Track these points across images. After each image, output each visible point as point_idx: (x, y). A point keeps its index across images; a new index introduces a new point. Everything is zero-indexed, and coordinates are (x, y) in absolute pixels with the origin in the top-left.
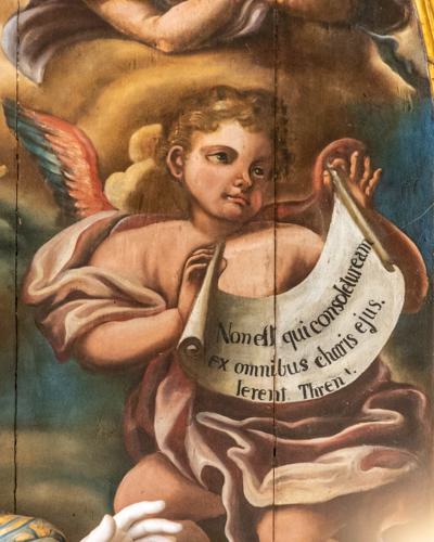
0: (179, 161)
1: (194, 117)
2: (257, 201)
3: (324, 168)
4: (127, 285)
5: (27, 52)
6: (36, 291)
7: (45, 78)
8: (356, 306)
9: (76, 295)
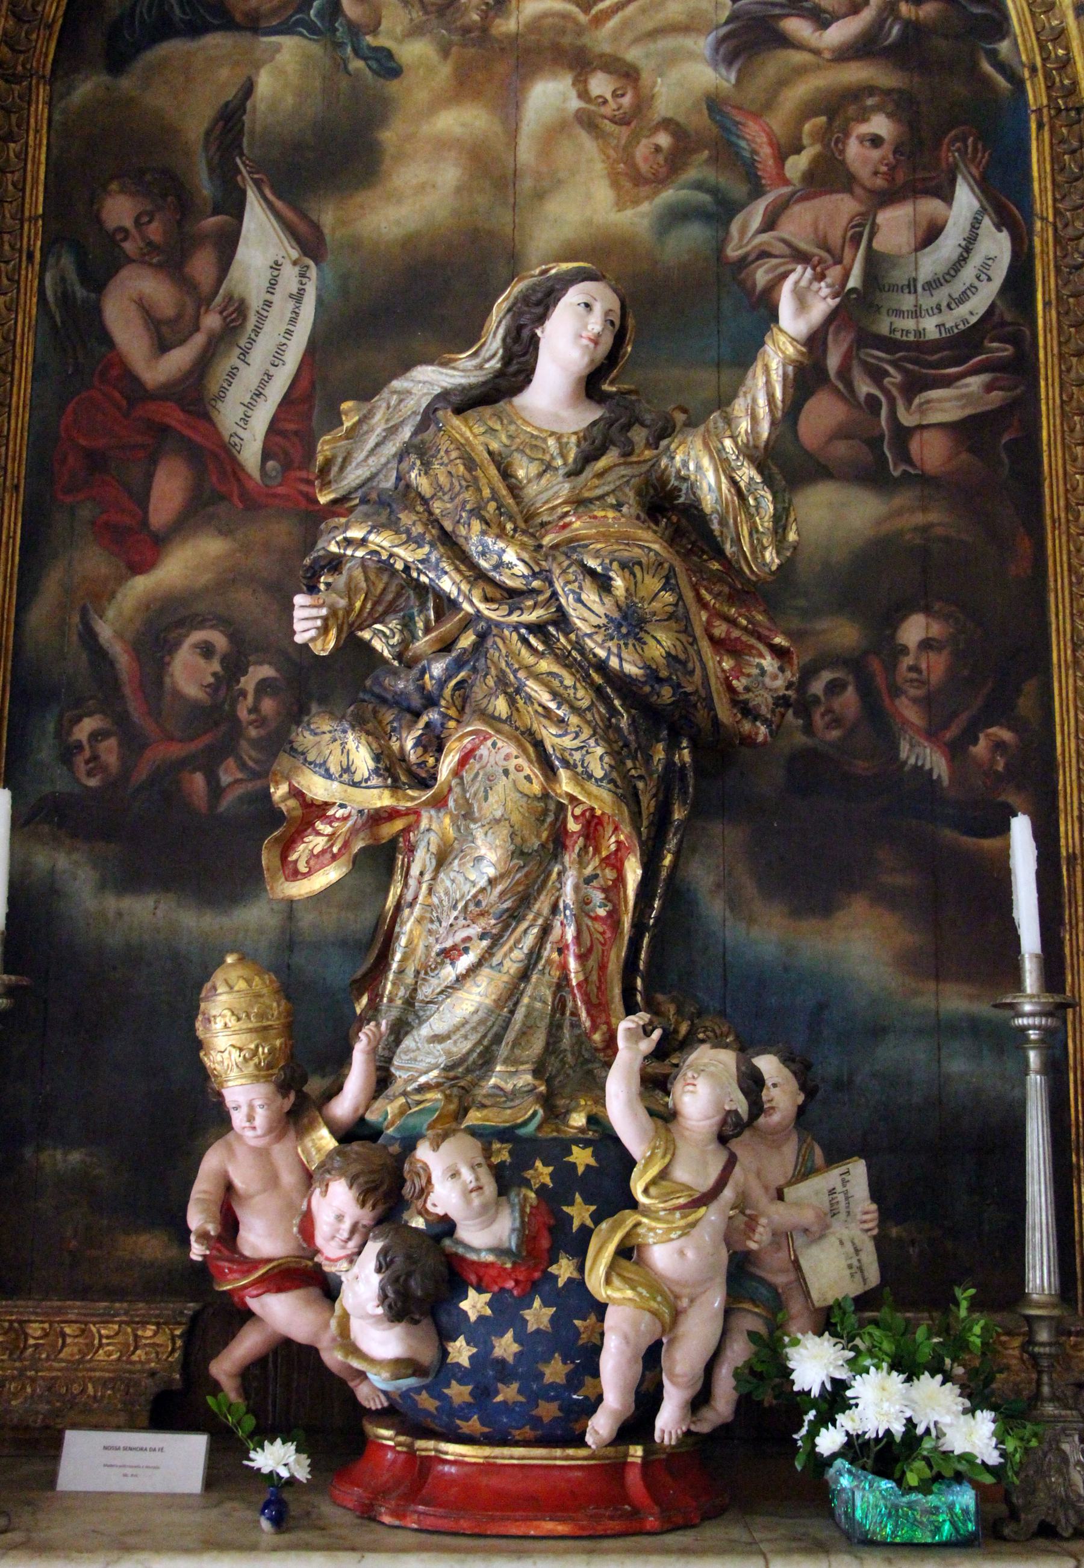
0: (840, 146)
1: (852, 110)
2: (901, 177)
3: (949, 150)
4: (803, 246)
5: (724, 60)
6: (733, 252)
7: (739, 80)
8: (976, 260)
9: (764, 254)
